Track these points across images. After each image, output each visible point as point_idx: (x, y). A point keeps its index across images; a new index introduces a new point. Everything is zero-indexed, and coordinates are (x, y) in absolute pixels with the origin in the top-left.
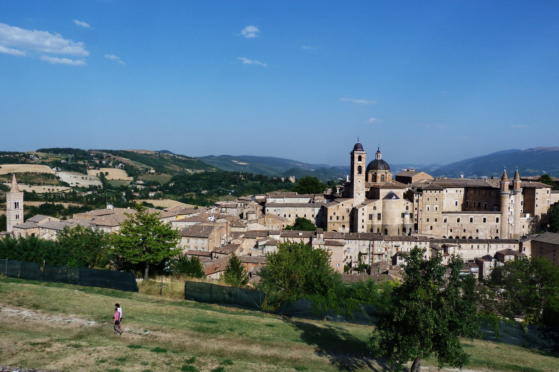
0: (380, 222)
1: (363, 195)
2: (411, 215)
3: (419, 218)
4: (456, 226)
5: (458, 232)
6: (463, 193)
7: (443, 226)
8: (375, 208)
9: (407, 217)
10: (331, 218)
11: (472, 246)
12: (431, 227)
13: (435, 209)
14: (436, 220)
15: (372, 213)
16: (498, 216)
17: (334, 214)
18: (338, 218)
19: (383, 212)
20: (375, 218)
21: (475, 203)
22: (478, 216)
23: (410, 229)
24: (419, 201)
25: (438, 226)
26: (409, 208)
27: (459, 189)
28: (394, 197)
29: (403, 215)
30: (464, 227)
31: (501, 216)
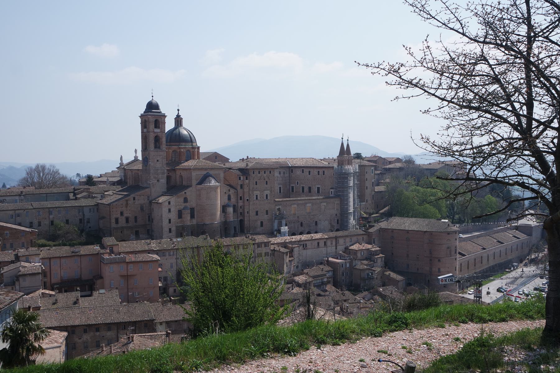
0: (194, 222)
1: (163, 181)
2: (234, 207)
3: (246, 211)
6: (287, 175)
8: (186, 200)
9: (230, 210)
10: (117, 220)
12: (262, 223)
17: (122, 214)
18: (127, 219)
20: (187, 216)
21: (303, 188)
23: (235, 228)
24: (245, 186)
26: (232, 197)
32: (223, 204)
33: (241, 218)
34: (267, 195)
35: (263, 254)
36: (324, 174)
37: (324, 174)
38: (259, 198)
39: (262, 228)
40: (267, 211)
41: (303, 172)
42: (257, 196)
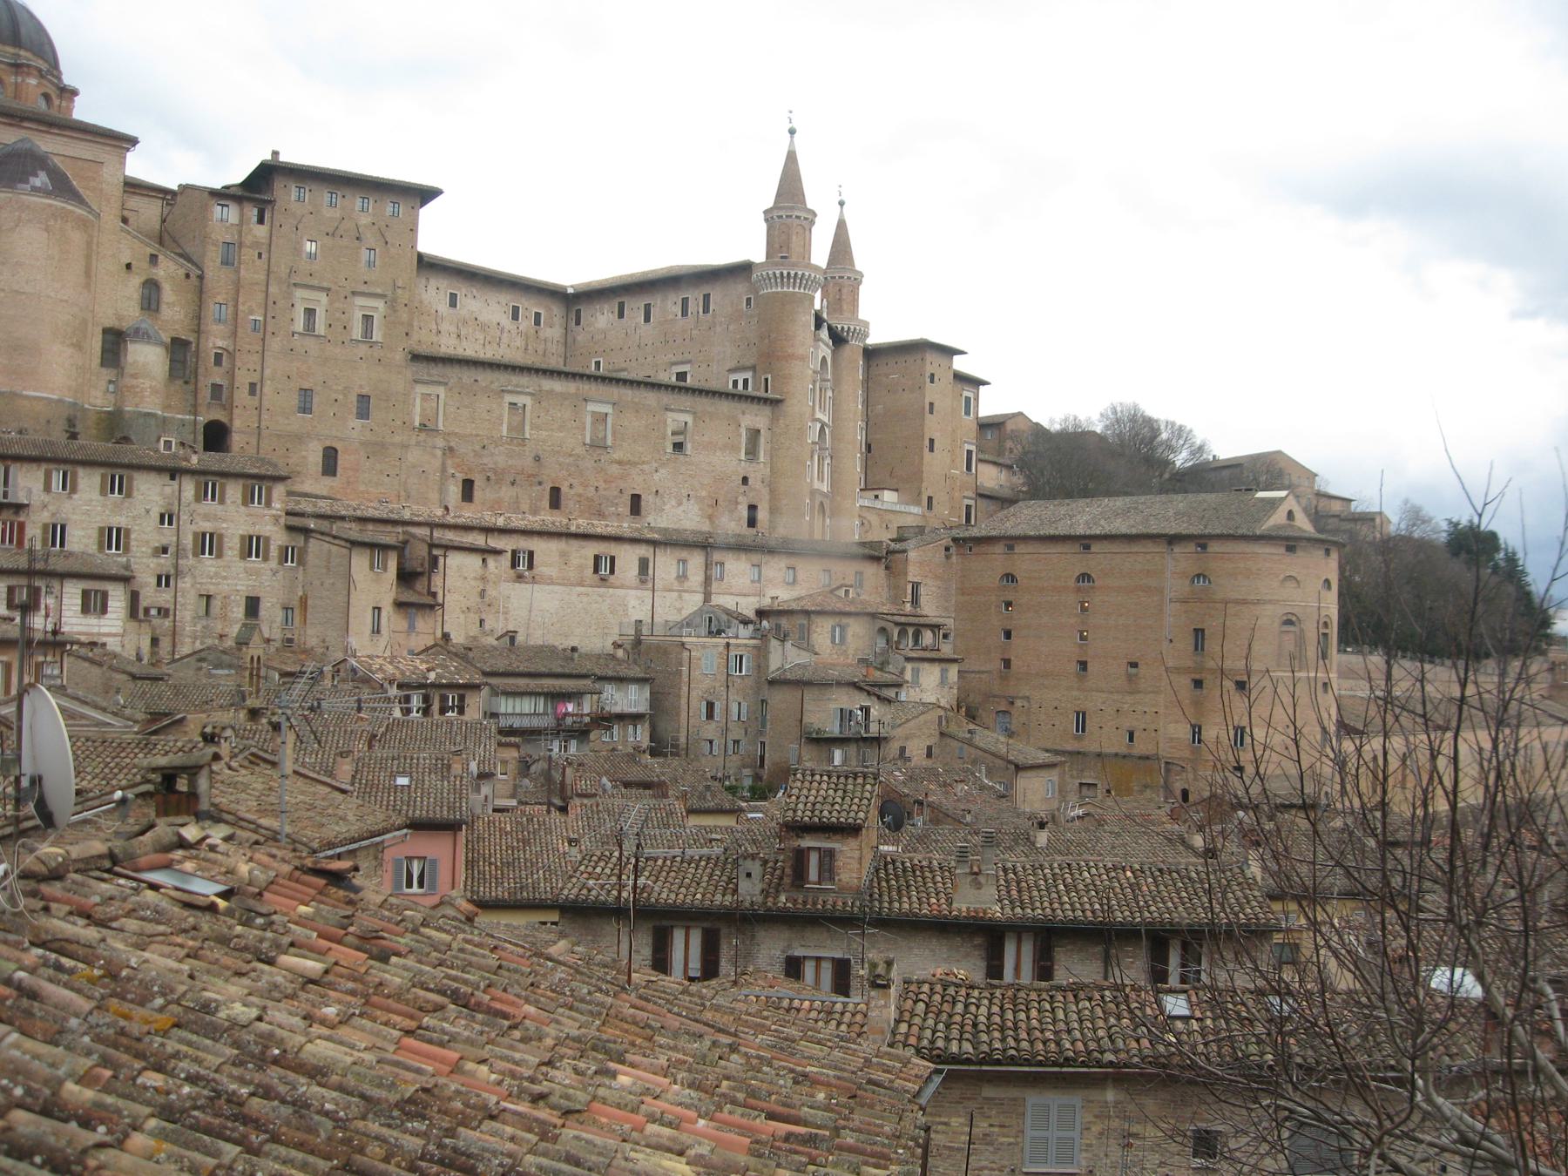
3: (243, 378)
4: (499, 458)
7: (413, 456)
9: (147, 358)
13: (357, 332)
14: (364, 406)
16: (755, 418)
24: (248, 254)
25: (377, 449)
26: (168, 294)
27: (530, 307)
28: (41, 180)
29: (115, 342)
30: (552, 473)
31: (774, 419)
32: (109, 323)
33: (218, 415)
34: (368, 319)
35: (232, 546)
36: (706, 310)
37: (706, 310)
38: (320, 328)
39: (328, 481)
40: (364, 399)
41: (621, 315)
42: (310, 313)
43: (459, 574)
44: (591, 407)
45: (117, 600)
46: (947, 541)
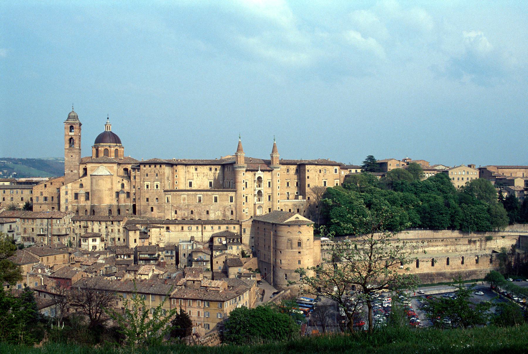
2: (128, 194)
3: (137, 198)
5: (184, 214)
6: (218, 172)
8: (81, 186)
9: (123, 196)
11: (182, 228)
15: (78, 192)
16: (232, 194)
17: (42, 194)
19: (91, 190)
20: (82, 199)
22: (207, 195)
26: (125, 185)
27: (213, 167)
38: (149, 188)
43: (154, 232)
44: (198, 196)
45: (98, 239)
46: (252, 220)
